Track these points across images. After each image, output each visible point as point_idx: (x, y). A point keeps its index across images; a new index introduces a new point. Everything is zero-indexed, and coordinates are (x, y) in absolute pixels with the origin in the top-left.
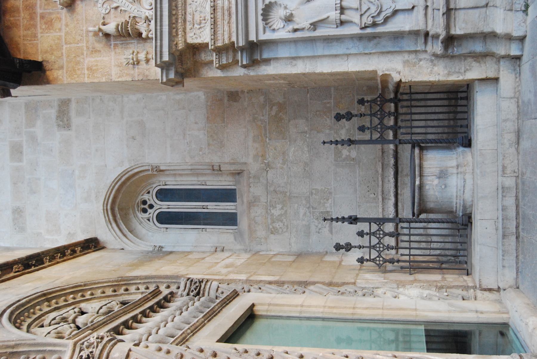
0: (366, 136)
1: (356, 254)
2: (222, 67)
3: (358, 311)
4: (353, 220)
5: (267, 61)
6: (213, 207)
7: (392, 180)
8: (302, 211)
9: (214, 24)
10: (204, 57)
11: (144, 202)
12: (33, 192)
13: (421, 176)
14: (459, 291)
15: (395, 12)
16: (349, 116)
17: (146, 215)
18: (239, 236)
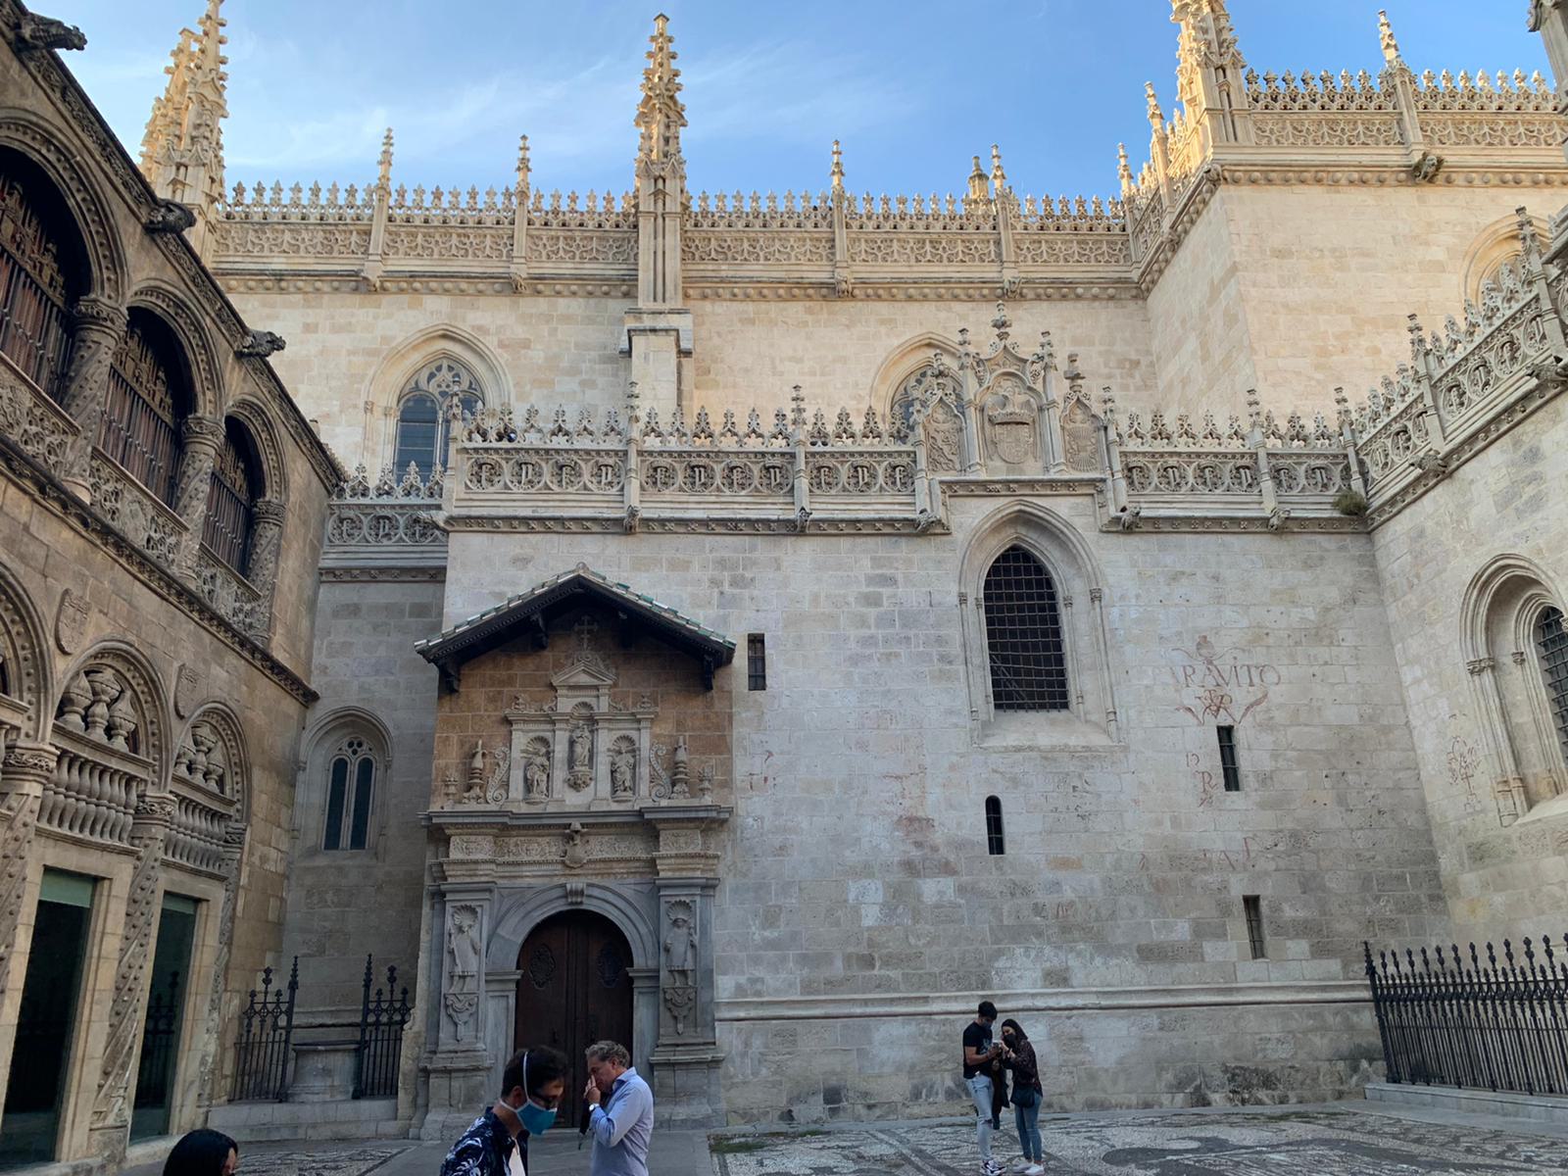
0: (373, 996)
1: (260, 986)
2: (431, 867)
3: (193, 998)
4: (293, 986)
5: (432, 907)
6: (347, 822)
7: (350, 1021)
8: (327, 924)
9: (463, 862)
10: (442, 849)
11: (360, 745)
12: (375, 627)
13: (326, 1051)
14: (207, 1090)
15: (456, 1024)
16: (392, 979)
17: (345, 747)
18: (312, 852)
